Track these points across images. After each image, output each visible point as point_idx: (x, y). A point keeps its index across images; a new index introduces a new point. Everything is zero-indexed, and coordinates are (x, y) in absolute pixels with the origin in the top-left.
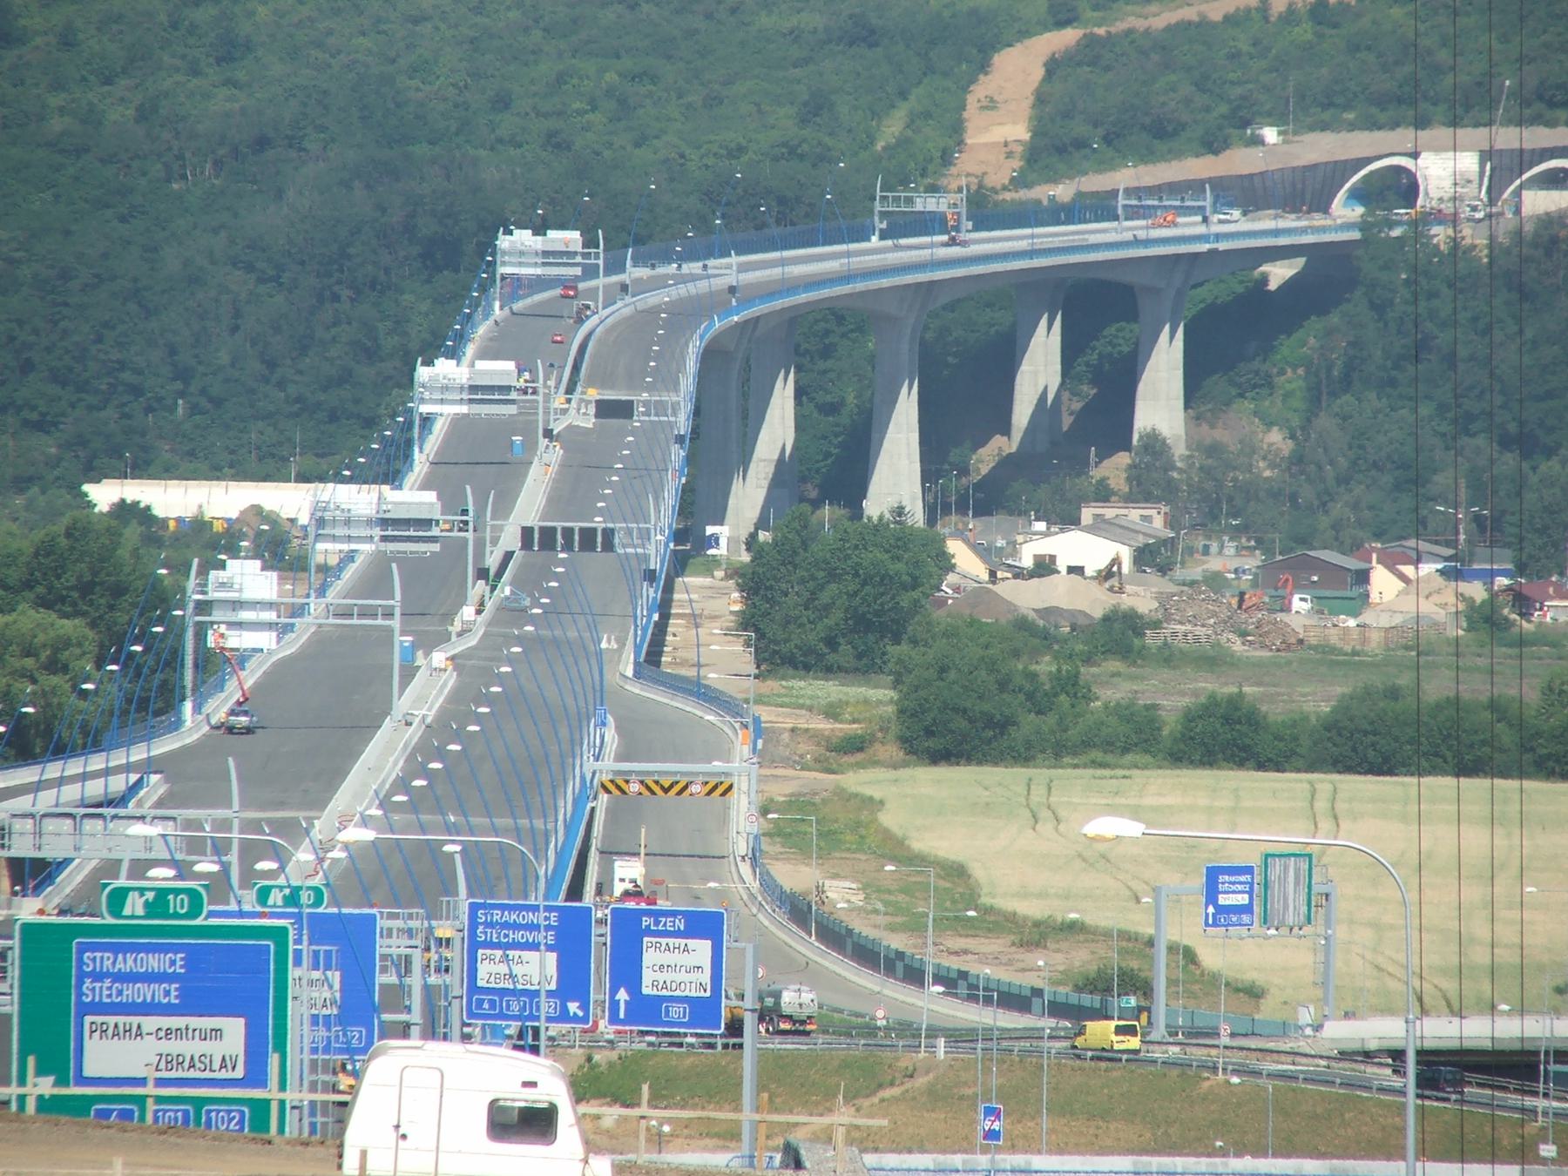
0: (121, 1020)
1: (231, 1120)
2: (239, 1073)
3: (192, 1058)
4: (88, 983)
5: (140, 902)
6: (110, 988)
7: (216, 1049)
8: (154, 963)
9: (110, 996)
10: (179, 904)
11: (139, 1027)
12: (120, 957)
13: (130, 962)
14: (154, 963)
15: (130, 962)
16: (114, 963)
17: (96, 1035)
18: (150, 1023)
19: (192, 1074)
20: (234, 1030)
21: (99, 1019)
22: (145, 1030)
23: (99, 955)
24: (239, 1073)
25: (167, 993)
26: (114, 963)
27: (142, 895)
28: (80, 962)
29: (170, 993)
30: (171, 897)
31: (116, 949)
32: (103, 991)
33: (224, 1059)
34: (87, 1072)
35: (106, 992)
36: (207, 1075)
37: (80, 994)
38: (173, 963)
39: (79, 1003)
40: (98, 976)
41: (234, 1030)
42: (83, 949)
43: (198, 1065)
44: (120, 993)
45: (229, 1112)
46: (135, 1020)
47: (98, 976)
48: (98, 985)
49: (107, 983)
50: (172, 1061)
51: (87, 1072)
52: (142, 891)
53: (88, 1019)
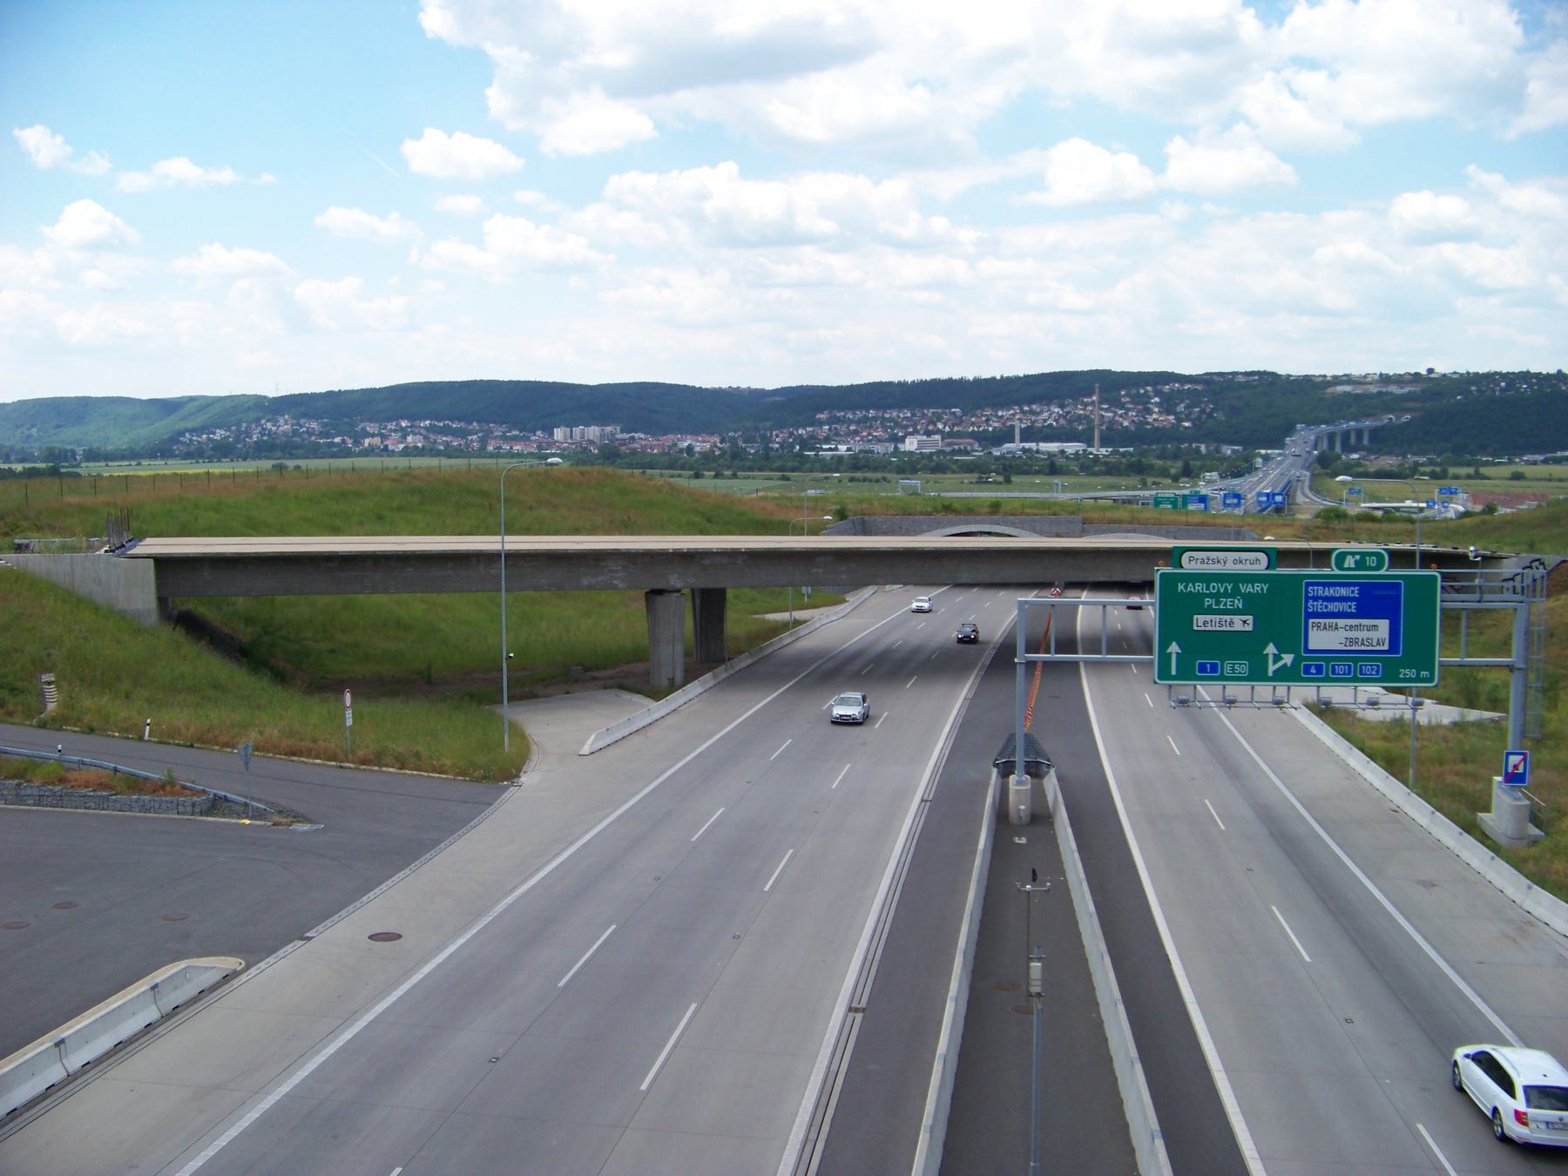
0: (1327, 621)
1: (1372, 670)
2: (1386, 647)
3: (1363, 640)
4: (1310, 602)
5: (1352, 561)
6: (1321, 605)
7: (1374, 635)
8: (1343, 592)
9: (1321, 609)
10: (1371, 561)
11: (1336, 624)
12: (1327, 589)
13: (1332, 591)
14: (1343, 592)
15: (1332, 591)
16: (1324, 592)
17: (1315, 629)
18: (1341, 622)
19: (1363, 648)
20: (1384, 625)
21: (1316, 621)
22: (1339, 626)
23: (1316, 588)
24: (1386, 647)
25: (1350, 607)
26: (1324, 592)
27: (1353, 557)
28: (1307, 592)
29: (1352, 607)
30: (1368, 558)
31: (1324, 585)
32: (1319, 606)
33: (1378, 640)
34: (1311, 647)
35: (1319, 607)
36: (1370, 648)
37: (1306, 607)
38: (1353, 592)
39: (1306, 611)
40: (1315, 599)
41: (1384, 625)
42: (1308, 584)
43: (1366, 643)
44: (1326, 607)
45: (1371, 665)
46: (1334, 621)
47: (1315, 599)
48: (1315, 603)
49: (1320, 602)
50: (1351, 641)
51: (1311, 647)
52: (1353, 554)
53: (1311, 621)
